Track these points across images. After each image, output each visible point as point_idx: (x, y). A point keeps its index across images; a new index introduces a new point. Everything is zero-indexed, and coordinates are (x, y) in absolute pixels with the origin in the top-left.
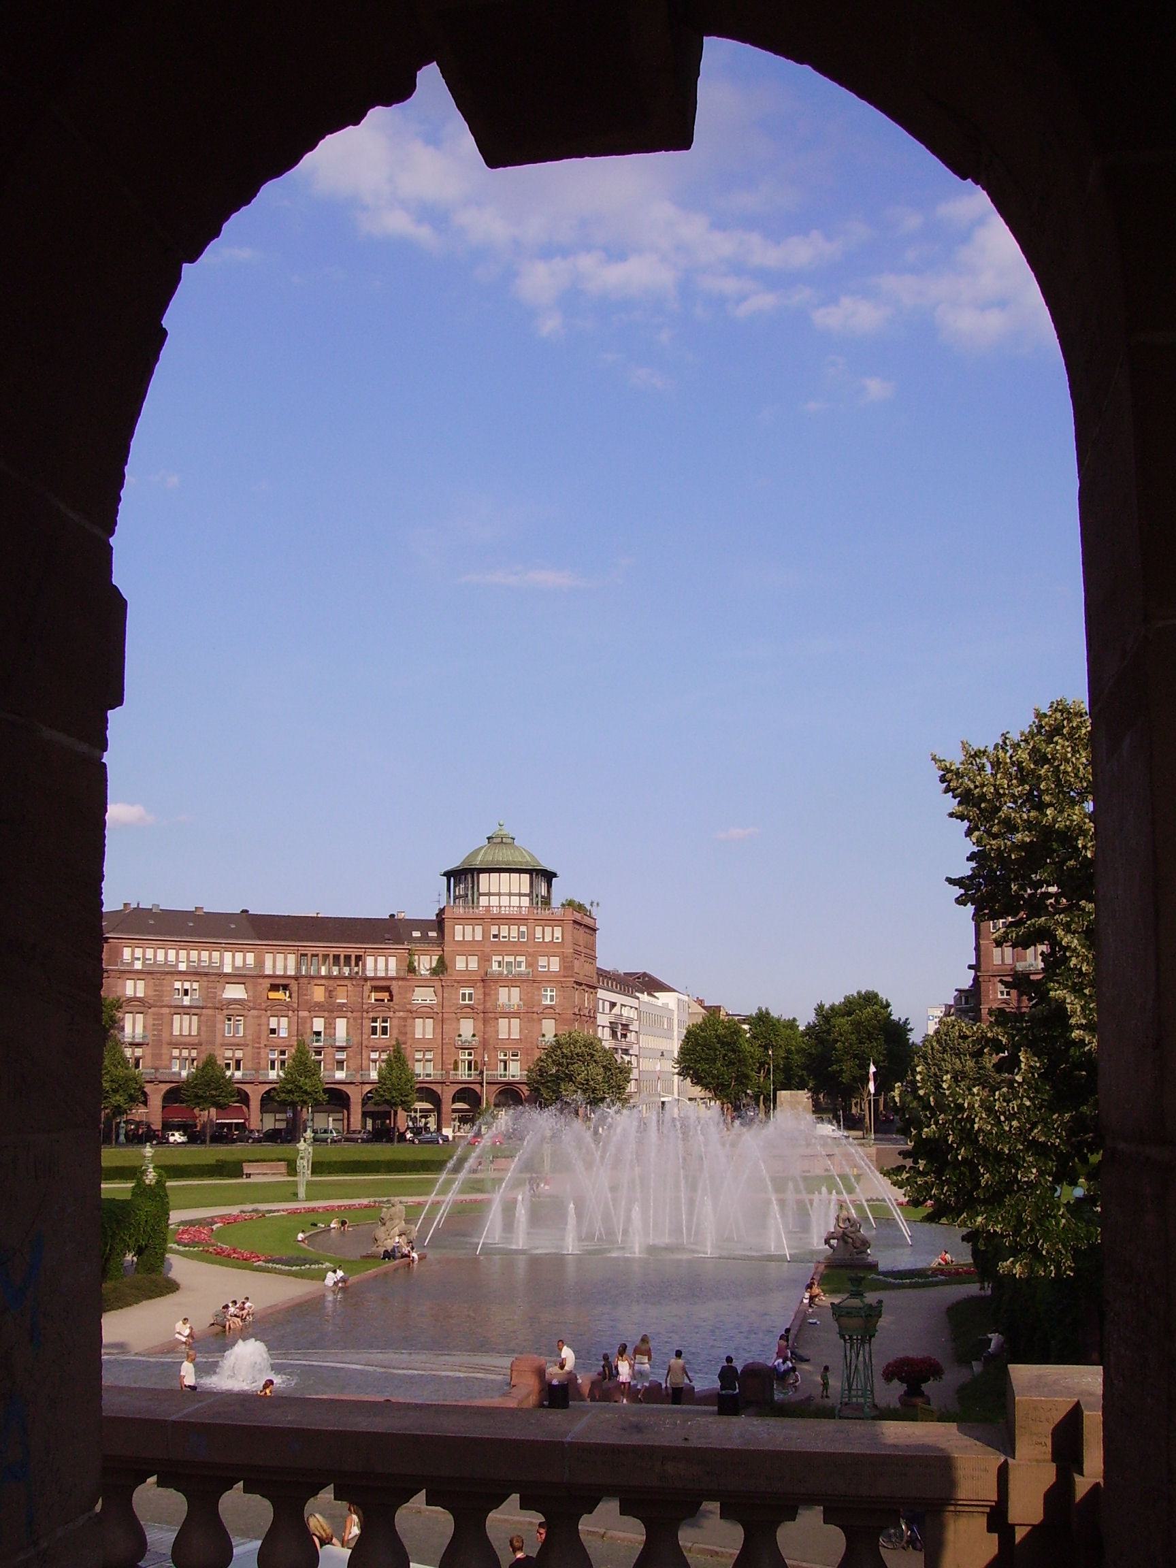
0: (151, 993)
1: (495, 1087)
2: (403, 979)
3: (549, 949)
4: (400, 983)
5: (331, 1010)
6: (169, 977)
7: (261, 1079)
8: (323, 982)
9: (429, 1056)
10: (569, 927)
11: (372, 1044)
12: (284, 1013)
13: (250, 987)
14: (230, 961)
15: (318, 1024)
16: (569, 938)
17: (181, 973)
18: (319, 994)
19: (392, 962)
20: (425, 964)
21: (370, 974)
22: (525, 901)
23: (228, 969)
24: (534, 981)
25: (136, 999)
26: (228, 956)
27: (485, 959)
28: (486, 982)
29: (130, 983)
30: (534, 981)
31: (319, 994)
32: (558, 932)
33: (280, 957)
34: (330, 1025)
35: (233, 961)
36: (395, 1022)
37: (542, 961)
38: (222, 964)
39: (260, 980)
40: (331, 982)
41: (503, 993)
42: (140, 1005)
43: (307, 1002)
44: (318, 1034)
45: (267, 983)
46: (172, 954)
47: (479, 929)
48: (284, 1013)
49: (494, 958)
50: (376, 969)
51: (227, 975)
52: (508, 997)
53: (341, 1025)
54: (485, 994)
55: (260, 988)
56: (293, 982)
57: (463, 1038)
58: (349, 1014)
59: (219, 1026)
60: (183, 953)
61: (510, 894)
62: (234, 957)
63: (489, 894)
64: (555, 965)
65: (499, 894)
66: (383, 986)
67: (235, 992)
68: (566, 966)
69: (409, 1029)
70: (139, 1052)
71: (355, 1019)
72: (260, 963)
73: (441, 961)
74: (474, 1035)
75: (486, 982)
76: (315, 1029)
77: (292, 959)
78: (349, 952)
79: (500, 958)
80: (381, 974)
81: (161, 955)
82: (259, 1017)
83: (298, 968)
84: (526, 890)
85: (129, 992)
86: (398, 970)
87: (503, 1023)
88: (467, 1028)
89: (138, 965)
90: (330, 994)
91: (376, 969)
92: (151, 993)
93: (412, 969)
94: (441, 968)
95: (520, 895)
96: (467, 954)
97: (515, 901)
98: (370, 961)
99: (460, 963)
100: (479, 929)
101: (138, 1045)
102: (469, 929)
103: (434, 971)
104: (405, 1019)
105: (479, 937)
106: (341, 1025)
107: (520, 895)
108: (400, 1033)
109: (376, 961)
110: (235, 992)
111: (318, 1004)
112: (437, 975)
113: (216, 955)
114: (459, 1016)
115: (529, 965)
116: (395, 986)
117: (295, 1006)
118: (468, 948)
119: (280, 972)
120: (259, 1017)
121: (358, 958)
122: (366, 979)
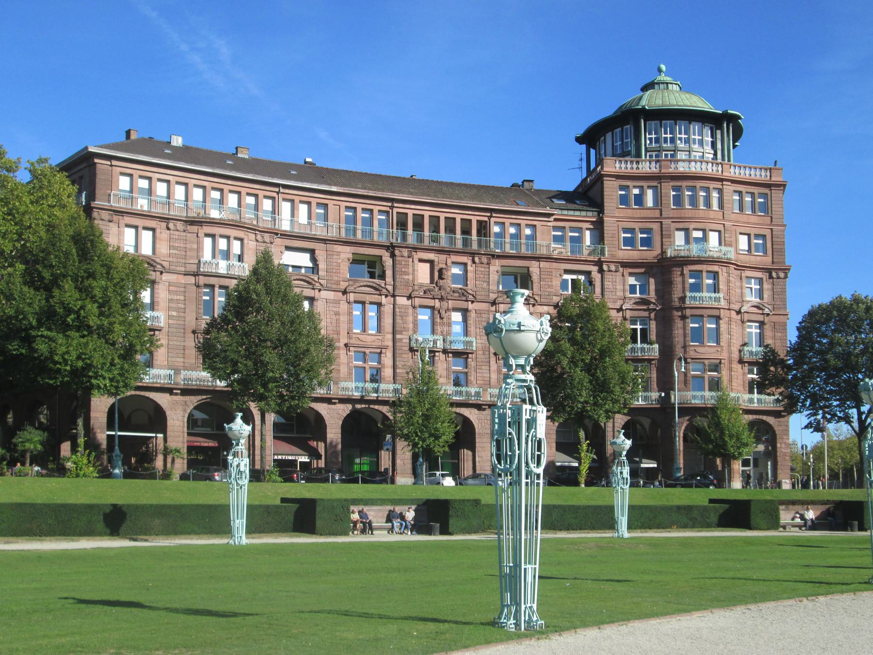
4: (543, 264)
7: (341, 394)
8: (431, 256)
12: (376, 298)
31: (423, 274)
43: (407, 284)
51: (284, 235)
82: (337, 302)
90: (438, 274)
92: (163, 249)
116: (535, 268)
117: (390, 288)
120: (337, 302)
122: (494, 256)
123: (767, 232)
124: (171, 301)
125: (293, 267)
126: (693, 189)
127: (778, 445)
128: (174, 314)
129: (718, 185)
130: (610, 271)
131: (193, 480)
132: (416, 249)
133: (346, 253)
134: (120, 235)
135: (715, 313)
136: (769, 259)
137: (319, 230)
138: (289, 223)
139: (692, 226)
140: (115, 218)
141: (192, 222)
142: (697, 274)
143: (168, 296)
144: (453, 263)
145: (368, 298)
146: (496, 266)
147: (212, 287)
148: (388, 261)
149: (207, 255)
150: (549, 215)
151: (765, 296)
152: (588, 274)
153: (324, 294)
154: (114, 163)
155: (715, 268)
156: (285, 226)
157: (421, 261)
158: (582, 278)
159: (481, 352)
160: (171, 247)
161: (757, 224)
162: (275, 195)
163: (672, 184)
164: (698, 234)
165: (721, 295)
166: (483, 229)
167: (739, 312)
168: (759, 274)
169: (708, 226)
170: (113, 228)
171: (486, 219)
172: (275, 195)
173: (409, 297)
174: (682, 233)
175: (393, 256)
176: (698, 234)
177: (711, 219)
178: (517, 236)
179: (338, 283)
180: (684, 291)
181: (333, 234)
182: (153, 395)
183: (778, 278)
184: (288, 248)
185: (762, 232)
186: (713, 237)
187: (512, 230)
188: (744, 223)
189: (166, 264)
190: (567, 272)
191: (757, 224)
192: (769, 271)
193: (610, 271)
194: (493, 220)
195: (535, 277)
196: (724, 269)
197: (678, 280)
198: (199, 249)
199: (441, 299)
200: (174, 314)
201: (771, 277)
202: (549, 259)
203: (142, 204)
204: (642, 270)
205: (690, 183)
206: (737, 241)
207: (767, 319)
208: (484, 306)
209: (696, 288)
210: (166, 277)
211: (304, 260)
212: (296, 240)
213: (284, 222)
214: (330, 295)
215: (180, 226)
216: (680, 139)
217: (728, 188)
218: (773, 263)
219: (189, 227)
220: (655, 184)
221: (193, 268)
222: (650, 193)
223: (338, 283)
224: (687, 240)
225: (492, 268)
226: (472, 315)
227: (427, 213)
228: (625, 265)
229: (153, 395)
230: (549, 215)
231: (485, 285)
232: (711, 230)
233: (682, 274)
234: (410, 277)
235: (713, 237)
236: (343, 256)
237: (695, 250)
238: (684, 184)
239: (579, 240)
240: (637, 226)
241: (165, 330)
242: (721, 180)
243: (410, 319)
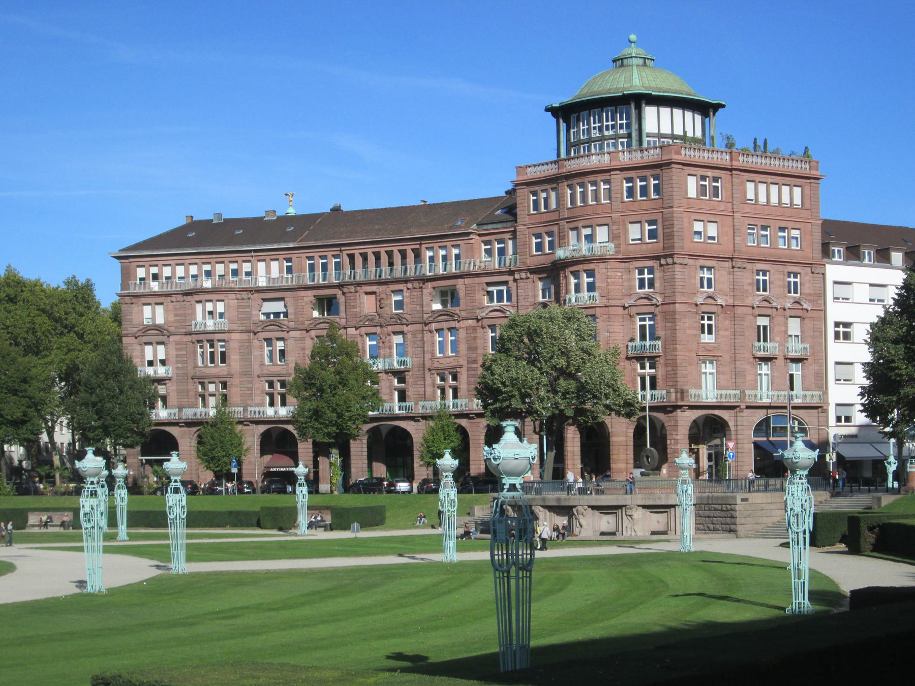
4: (467, 281)
8: (373, 288)
11: (436, 365)
14: (267, 272)
18: (368, 305)
29: (147, 310)
42: (157, 333)
43: (355, 316)
59: (256, 353)
71: (414, 333)
82: (303, 339)
92: (171, 318)
104: (474, 329)
115: (613, 237)
120: (303, 339)
123: (659, 217)
124: (177, 356)
125: (274, 313)
126: (582, 185)
127: (668, 442)
128: (180, 365)
129: (605, 176)
130: (521, 279)
131: (554, 468)
132: (359, 284)
133: (309, 296)
135: (590, 312)
136: (661, 245)
137: (289, 280)
138: (264, 279)
139: (580, 224)
140: (134, 300)
141: (187, 294)
142: (576, 275)
143: (175, 353)
144: (393, 291)
146: (429, 287)
147: (201, 341)
148: (341, 299)
149: (199, 317)
150: (468, 234)
151: (657, 285)
152: (505, 283)
153: (292, 334)
154: (131, 260)
155: (591, 266)
156: (262, 282)
157: (367, 293)
158: (504, 288)
159: (416, 369)
160: (176, 315)
161: (651, 209)
162: (250, 258)
163: (565, 183)
164: (588, 231)
165: (596, 294)
166: (417, 255)
167: (625, 308)
168: (650, 263)
169: (594, 222)
170: (135, 308)
171: (418, 246)
172: (250, 258)
173: (357, 329)
174: (575, 232)
175: (344, 294)
176: (588, 231)
177: (599, 214)
178: (445, 258)
179: (303, 323)
180: (568, 292)
181: (295, 283)
182: (167, 429)
183: (667, 264)
184: (265, 300)
185: (653, 217)
186: (602, 234)
187: (442, 252)
188: (636, 211)
189: (172, 329)
190: (488, 284)
191: (651, 209)
192: (657, 258)
193: (521, 279)
194: (424, 246)
195: (462, 294)
196: (602, 265)
197: (563, 282)
199: (381, 326)
200: (180, 365)
201: (661, 265)
202: (469, 275)
203: (155, 286)
204: (544, 275)
205: (580, 180)
206: (626, 232)
207: (657, 311)
209: (578, 289)
210: (172, 338)
211: (278, 307)
212: (273, 292)
213: (260, 279)
214: (296, 334)
215: (180, 298)
216: (594, 128)
217: (617, 177)
218: (664, 248)
219: (185, 298)
220: (554, 185)
221: (188, 329)
222: (553, 195)
223: (303, 323)
224: (579, 239)
225: (425, 291)
226: (409, 336)
227: (370, 251)
228: (533, 271)
229: (167, 429)
230: (468, 234)
231: (419, 308)
232: (598, 225)
233: (566, 277)
234: (358, 310)
235: (602, 234)
236: (306, 299)
237: (584, 249)
238: (575, 181)
239: (502, 252)
240: (542, 230)
241: (175, 378)
242: (609, 171)
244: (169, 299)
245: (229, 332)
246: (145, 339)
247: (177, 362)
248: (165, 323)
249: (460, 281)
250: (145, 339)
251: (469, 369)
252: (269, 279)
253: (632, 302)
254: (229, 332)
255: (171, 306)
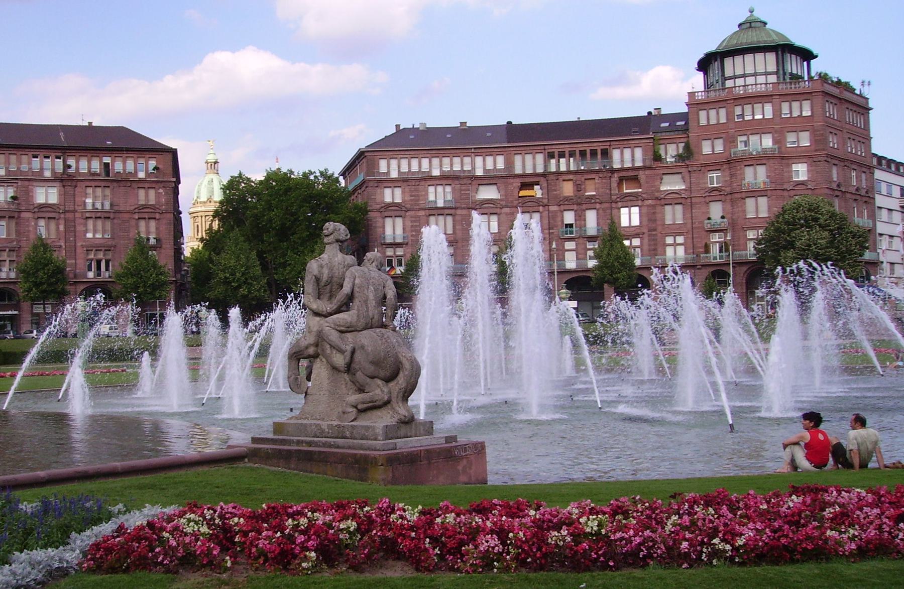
0: (407, 198)
1: (745, 268)
2: (650, 168)
3: (799, 124)
4: (647, 172)
5: (580, 204)
6: (422, 183)
8: (571, 177)
9: (680, 240)
10: (819, 100)
12: (535, 209)
13: (502, 187)
14: (480, 165)
15: (569, 217)
16: (818, 111)
17: (436, 178)
18: (568, 189)
19: (638, 153)
20: (670, 152)
21: (617, 166)
22: (773, 79)
23: (479, 172)
24: (783, 158)
25: (393, 204)
26: (479, 160)
27: (730, 141)
28: (731, 163)
30: (783, 158)
31: (568, 189)
32: (807, 105)
33: (529, 157)
34: (581, 217)
35: (484, 164)
36: (645, 210)
37: (791, 137)
38: (474, 168)
39: (511, 180)
40: (579, 177)
41: (749, 173)
44: (571, 226)
45: (517, 183)
46: (425, 162)
47: (723, 112)
48: (535, 209)
49: (740, 139)
50: (622, 161)
52: (756, 176)
53: (591, 218)
54: (732, 175)
55: (511, 187)
56: (542, 179)
57: (712, 222)
58: (598, 206)
60: (436, 161)
61: (755, 75)
62: (484, 160)
63: (735, 77)
64: (805, 140)
65: (744, 76)
66: (630, 176)
67: (488, 193)
68: (819, 140)
69: (658, 216)
70: (400, 252)
71: (604, 210)
72: (509, 163)
73: (687, 147)
74: (723, 217)
75: (731, 163)
76: (566, 222)
77: (540, 158)
78: (594, 146)
79: (744, 138)
80: (628, 165)
81: (415, 163)
83: (546, 166)
84: (772, 67)
85: (388, 199)
86: (644, 161)
87: (750, 203)
88: (716, 211)
89: (394, 175)
90: (578, 188)
91: (622, 161)
92: (407, 198)
93: (657, 158)
94: (687, 155)
95: (766, 74)
96: (712, 138)
97: (761, 79)
98: (616, 154)
99: (706, 148)
100: (723, 112)
101: (399, 245)
102: (713, 113)
103: (679, 157)
104: (654, 206)
105: (723, 120)
106: (591, 218)
107: (766, 74)
108: (650, 220)
109: (622, 154)
110: (488, 193)
111: (567, 199)
112: (683, 161)
113: (467, 160)
114: (708, 199)
118: (713, 132)
119: (529, 171)
121: (606, 153)
122: (613, 171)
134: (383, 193)
145: (531, 209)
170: (379, 190)
189: (408, 206)
198: (427, 194)
208: (607, 205)
223: (512, 202)
225: (612, 179)
231: (608, 191)
234: (558, 192)
243: (559, 219)
244: (405, 184)
245: (456, 208)
246: (386, 214)
247: (412, 231)
248: (404, 201)
249: (641, 172)
250: (386, 214)
251: (649, 235)
252: (485, 170)
253: (791, 187)
254: (456, 208)
255: (407, 189)
